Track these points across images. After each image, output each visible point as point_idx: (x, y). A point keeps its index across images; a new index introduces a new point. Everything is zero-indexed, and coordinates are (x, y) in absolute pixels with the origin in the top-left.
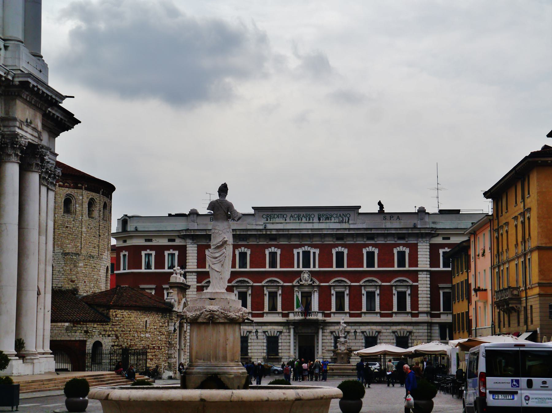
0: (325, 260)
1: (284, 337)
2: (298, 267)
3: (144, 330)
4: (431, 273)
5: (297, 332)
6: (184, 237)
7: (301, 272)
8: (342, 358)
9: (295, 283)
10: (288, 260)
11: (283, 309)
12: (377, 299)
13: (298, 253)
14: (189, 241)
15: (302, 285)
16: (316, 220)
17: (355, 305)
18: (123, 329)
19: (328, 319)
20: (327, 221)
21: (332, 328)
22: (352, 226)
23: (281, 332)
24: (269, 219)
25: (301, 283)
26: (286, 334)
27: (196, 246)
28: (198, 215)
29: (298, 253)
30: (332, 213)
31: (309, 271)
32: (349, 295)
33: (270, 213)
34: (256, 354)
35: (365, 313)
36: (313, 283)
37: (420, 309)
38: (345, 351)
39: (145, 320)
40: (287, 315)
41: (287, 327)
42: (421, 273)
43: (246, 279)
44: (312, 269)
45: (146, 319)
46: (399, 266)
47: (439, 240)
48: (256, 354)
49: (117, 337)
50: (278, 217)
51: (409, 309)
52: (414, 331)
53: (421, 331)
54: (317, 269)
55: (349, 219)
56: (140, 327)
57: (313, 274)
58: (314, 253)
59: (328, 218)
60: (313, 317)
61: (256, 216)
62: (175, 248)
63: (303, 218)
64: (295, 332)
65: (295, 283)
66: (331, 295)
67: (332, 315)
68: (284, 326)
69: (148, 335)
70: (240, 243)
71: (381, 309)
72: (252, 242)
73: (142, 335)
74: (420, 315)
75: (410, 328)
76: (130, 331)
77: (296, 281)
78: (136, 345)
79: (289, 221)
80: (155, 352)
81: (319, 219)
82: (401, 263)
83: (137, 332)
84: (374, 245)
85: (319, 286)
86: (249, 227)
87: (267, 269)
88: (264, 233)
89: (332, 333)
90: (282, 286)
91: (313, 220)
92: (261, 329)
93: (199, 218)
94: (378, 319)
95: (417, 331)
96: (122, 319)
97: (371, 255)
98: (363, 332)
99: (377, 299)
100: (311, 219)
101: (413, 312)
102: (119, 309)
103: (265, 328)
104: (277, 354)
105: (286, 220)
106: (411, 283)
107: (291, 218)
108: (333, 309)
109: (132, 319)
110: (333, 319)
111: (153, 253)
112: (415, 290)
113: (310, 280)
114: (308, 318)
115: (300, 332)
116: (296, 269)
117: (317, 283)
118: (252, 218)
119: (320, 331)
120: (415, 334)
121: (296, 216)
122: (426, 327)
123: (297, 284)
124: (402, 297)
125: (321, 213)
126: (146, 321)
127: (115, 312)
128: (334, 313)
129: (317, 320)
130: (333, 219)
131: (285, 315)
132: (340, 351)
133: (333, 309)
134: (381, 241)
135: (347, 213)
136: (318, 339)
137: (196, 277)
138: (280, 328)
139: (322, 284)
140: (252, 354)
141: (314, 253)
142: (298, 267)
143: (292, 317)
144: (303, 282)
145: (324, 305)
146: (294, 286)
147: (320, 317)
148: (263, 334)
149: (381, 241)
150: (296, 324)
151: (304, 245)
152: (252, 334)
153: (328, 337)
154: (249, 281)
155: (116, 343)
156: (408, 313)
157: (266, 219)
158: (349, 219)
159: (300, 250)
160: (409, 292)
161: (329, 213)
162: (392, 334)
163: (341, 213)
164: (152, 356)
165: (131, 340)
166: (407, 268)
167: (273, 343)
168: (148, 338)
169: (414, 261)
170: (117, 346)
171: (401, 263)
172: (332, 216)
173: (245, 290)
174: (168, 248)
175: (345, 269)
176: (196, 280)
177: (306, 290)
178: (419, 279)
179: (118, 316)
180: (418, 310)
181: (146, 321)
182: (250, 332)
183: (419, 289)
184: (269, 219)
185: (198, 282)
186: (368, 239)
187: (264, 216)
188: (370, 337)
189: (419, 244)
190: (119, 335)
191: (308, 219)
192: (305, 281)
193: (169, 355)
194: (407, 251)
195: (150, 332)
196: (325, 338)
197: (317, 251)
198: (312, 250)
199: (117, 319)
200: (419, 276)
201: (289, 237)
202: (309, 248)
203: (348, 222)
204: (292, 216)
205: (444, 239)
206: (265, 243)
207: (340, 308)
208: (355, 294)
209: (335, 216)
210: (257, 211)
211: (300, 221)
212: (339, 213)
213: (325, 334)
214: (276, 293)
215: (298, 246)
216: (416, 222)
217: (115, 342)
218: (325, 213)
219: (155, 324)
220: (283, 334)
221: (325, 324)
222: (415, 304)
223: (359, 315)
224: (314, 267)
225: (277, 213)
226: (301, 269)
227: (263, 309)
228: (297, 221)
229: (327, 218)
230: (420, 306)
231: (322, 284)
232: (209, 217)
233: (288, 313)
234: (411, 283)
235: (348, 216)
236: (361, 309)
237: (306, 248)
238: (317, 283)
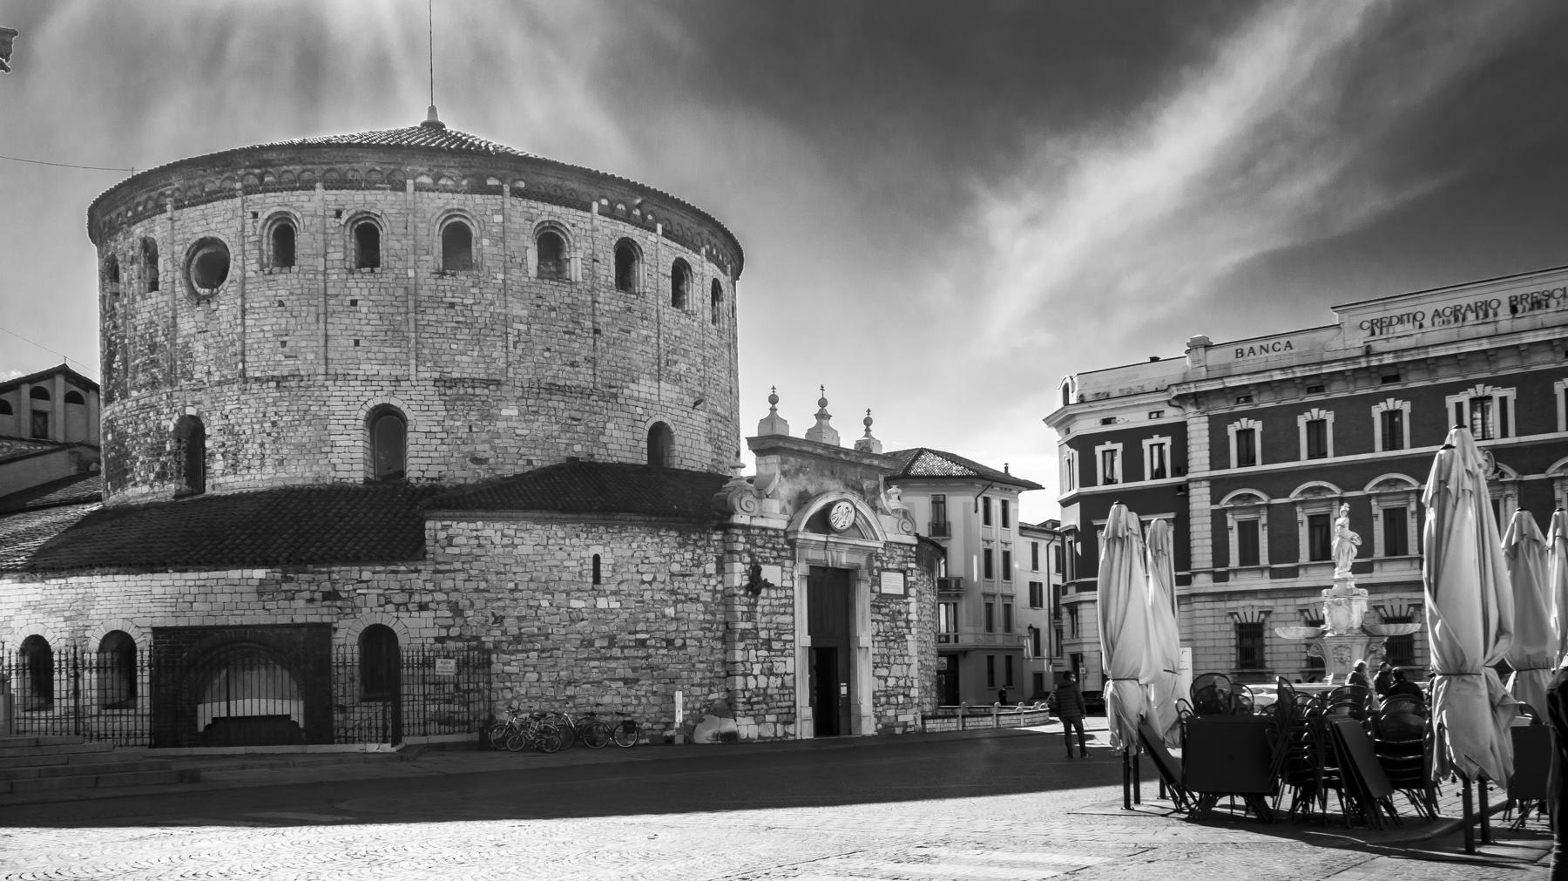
6: (1181, 401)
13: (1459, 406)
14: (1191, 410)
16: (1504, 311)
18: (483, 585)
24: (1377, 331)
29: (1459, 406)
36: (1502, 475)
43: (1325, 484)
45: (597, 550)
49: (457, 610)
50: (1401, 320)
54: (1512, 439)
58: (1503, 400)
62: (1162, 430)
70: (1307, 400)
76: (516, 589)
78: (547, 637)
80: (649, 656)
83: (546, 591)
88: (1364, 365)
91: (1496, 315)
96: (477, 551)
100: (1491, 312)
102: (460, 519)
105: (1421, 326)
109: (523, 550)
121: (1448, 312)
126: (597, 558)
127: (444, 528)
130: (1553, 302)
137: (1208, 490)
139: (1527, 478)
141: (1503, 400)
151: (1473, 384)
154: (1332, 487)
155: (454, 632)
157: (1368, 332)
159: (1464, 397)
164: (634, 670)
165: (520, 619)
170: (460, 638)
173: (1322, 510)
174: (1148, 432)
179: (455, 541)
181: (597, 558)
185: (1213, 502)
187: (1366, 325)
190: (463, 603)
191: (1481, 314)
193: (729, 667)
195: (614, 593)
197: (1511, 393)
198: (1497, 393)
199: (456, 551)
201: (1429, 365)
202: (1489, 388)
206: (1370, 391)
209: (1558, 294)
214: (1403, 510)
215: (1456, 388)
217: (448, 628)
219: (643, 568)
229: (1537, 304)
231: (1527, 478)
237: (1480, 390)
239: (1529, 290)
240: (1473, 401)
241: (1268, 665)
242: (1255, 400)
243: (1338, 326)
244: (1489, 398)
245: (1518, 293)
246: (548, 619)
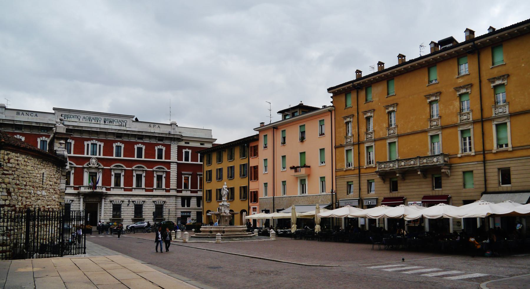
0: (108, 150)
1: (74, 205)
2: (88, 154)
3: (41, 185)
4: (178, 164)
7: (90, 158)
8: (226, 220)
9: (85, 166)
11: (74, 184)
12: (143, 179)
13: (88, 145)
15: (90, 167)
16: (102, 122)
17: (128, 182)
18: (18, 182)
19: (109, 192)
21: (112, 198)
22: (128, 129)
23: (73, 201)
26: (77, 202)
28: (6, 109)
29: (88, 145)
30: (115, 119)
31: (97, 158)
32: (124, 176)
33: (67, 114)
35: (135, 188)
38: (229, 214)
39: (42, 172)
41: (77, 197)
44: (98, 156)
46: (158, 158)
47: (182, 144)
49: (9, 193)
51: (164, 187)
52: (167, 201)
54: (102, 156)
56: (37, 181)
57: (99, 159)
58: (100, 145)
60: (98, 190)
61: (56, 115)
64: (84, 201)
65: (85, 166)
66: (111, 175)
69: (44, 193)
71: (146, 186)
73: (39, 193)
74: (171, 191)
75: (164, 199)
76: (26, 185)
77: (86, 164)
81: (105, 122)
82: (160, 157)
84: (142, 143)
85: (102, 169)
86: (50, 122)
89: (111, 201)
90: (75, 167)
93: (6, 111)
94: (143, 193)
96: (17, 167)
97: (140, 149)
98: (133, 202)
99: (143, 179)
102: (13, 152)
104: (141, 216)
106: (166, 170)
108: (113, 185)
109: (29, 168)
110: (112, 192)
112: (168, 174)
114: (95, 191)
116: (85, 155)
117: (102, 167)
118: (53, 116)
119: (103, 200)
122: (174, 199)
124: (159, 178)
125: (106, 118)
127: (8, 154)
128: (113, 188)
129: (103, 192)
131: (75, 188)
132: (224, 214)
133: (113, 185)
134: (147, 141)
135: (125, 119)
136: (101, 206)
138: (72, 198)
141: (100, 145)
142: (88, 154)
143: (82, 190)
144: (91, 165)
145: (106, 182)
147: (104, 190)
149: (147, 141)
150: (85, 195)
151: (92, 139)
153: (108, 205)
155: (7, 202)
156: (163, 189)
160: (164, 175)
161: (112, 118)
162: (152, 203)
163: (121, 119)
165: (27, 198)
166: (163, 160)
168: (43, 196)
169: (168, 156)
170: (9, 206)
171: (160, 157)
172: (114, 121)
175: (122, 157)
177: (93, 171)
179: (11, 161)
186: (139, 139)
188: (116, 205)
190: (11, 190)
192: (93, 164)
194: (164, 149)
197: (102, 144)
198: (99, 143)
199: (10, 165)
205: (186, 143)
207: (117, 184)
208: (129, 176)
210: (57, 111)
212: (119, 119)
213: (106, 203)
215: (88, 140)
216: (170, 130)
217: (5, 200)
218: (109, 118)
222: (168, 184)
223: (131, 190)
224: (100, 155)
225: (73, 114)
226: (89, 156)
229: (110, 122)
232: (16, 112)
233: (80, 187)
234: (166, 170)
236: (132, 186)
237: (94, 142)
238: (102, 167)
239: (109, 118)
240: (92, 144)
241: (122, 217)
242: (23, 130)
243: (54, 114)
244: (96, 144)
245: (106, 118)
246: (33, 199)
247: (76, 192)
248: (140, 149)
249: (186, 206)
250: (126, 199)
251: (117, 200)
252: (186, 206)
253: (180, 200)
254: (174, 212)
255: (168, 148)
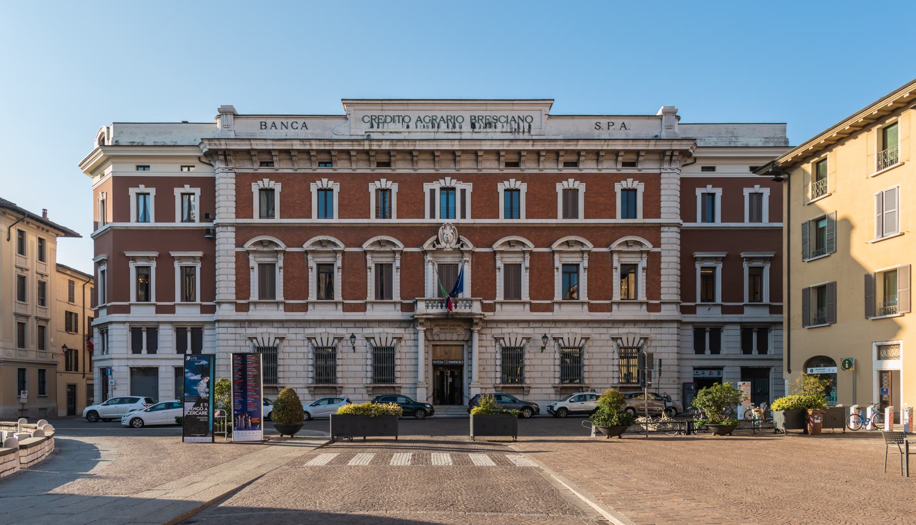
1: (405, 349)
2: (433, 216)
5: (430, 338)
9: (427, 246)
10: (412, 202)
12: (583, 277)
13: (433, 192)
15: (440, 251)
16: (467, 127)
19: (489, 315)
20: (489, 130)
21: (497, 332)
23: (399, 339)
24: (375, 125)
25: (438, 246)
27: (233, 175)
28: (236, 116)
29: (433, 192)
34: (351, 381)
36: (462, 246)
37: (662, 297)
40: (411, 307)
41: (411, 330)
42: (666, 229)
43: (332, 239)
44: (458, 220)
48: (351, 381)
50: (393, 120)
53: (664, 337)
54: (469, 220)
55: (530, 127)
57: (461, 230)
58: (463, 192)
59: (490, 124)
60: (461, 309)
63: (442, 123)
64: (426, 339)
67: (498, 307)
68: (405, 328)
71: (590, 296)
72: (342, 167)
75: (645, 331)
77: (429, 241)
79: (415, 130)
82: (629, 211)
85: (472, 253)
87: (373, 220)
89: (497, 340)
91: (461, 128)
92: (360, 333)
93: (238, 121)
95: (658, 337)
97: (571, 194)
99: (583, 277)
100: (457, 125)
101: (651, 302)
103: (368, 331)
105: (408, 127)
106: (648, 246)
107: (419, 123)
108: (500, 297)
111: (152, 191)
112: (654, 260)
113: (455, 241)
115: (436, 338)
116: (427, 220)
119: (476, 336)
120: (654, 344)
121: (427, 119)
122: (675, 331)
123: (431, 248)
130: (499, 125)
137: (233, 235)
138: (399, 332)
139: (477, 250)
140: (345, 381)
141: (463, 192)
142: (433, 216)
144: (443, 244)
145: (484, 288)
146: (425, 252)
147: (476, 308)
148: (365, 342)
151: (443, 176)
152: (344, 343)
157: (369, 125)
158: (530, 127)
159: (436, 186)
160: (643, 263)
162: (611, 343)
166: (640, 219)
167: (383, 361)
169: (653, 208)
171: (629, 211)
176: (234, 241)
177: (449, 260)
178: (662, 241)
180: (659, 299)
182: (340, 339)
183: (663, 259)
184: (375, 125)
187: (367, 119)
189: (662, 175)
191: (451, 125)
192: (447, 242)
194: (640, 188)
196: (483, 349)
197: (469, 187)
198: (459, 186)
200: (663, 235)
203: (529, 132)
204: (419, 119)
206: (368, 171)
207: (512, 293)
209: (503, 119)
211: (436, 129)
213: (484, 343)
220: (403, 343)
221: (487, 323)
222: (654, 289)
223: (549, 308)
224: (463, 216)
226: (437, 220)
227: (364, 295)
228: (430, 129)
229: (488, 125)
230: (663, 291)
235: (529, 119)
236: (552, 296)
237: (448, 182)
238: (470, 246)
239: (484, 114)
240: (442, 189)
242: (276, 165)
243: (345, 117)
245: (477, 114)
247: (407, 315)
248: (571, 194)
249: (708, 351)
250: (536, 333)
251: (513, 336)
252: (708, 351)
253: (689, 332)
254: (676, 368)
255: (653, 183)
